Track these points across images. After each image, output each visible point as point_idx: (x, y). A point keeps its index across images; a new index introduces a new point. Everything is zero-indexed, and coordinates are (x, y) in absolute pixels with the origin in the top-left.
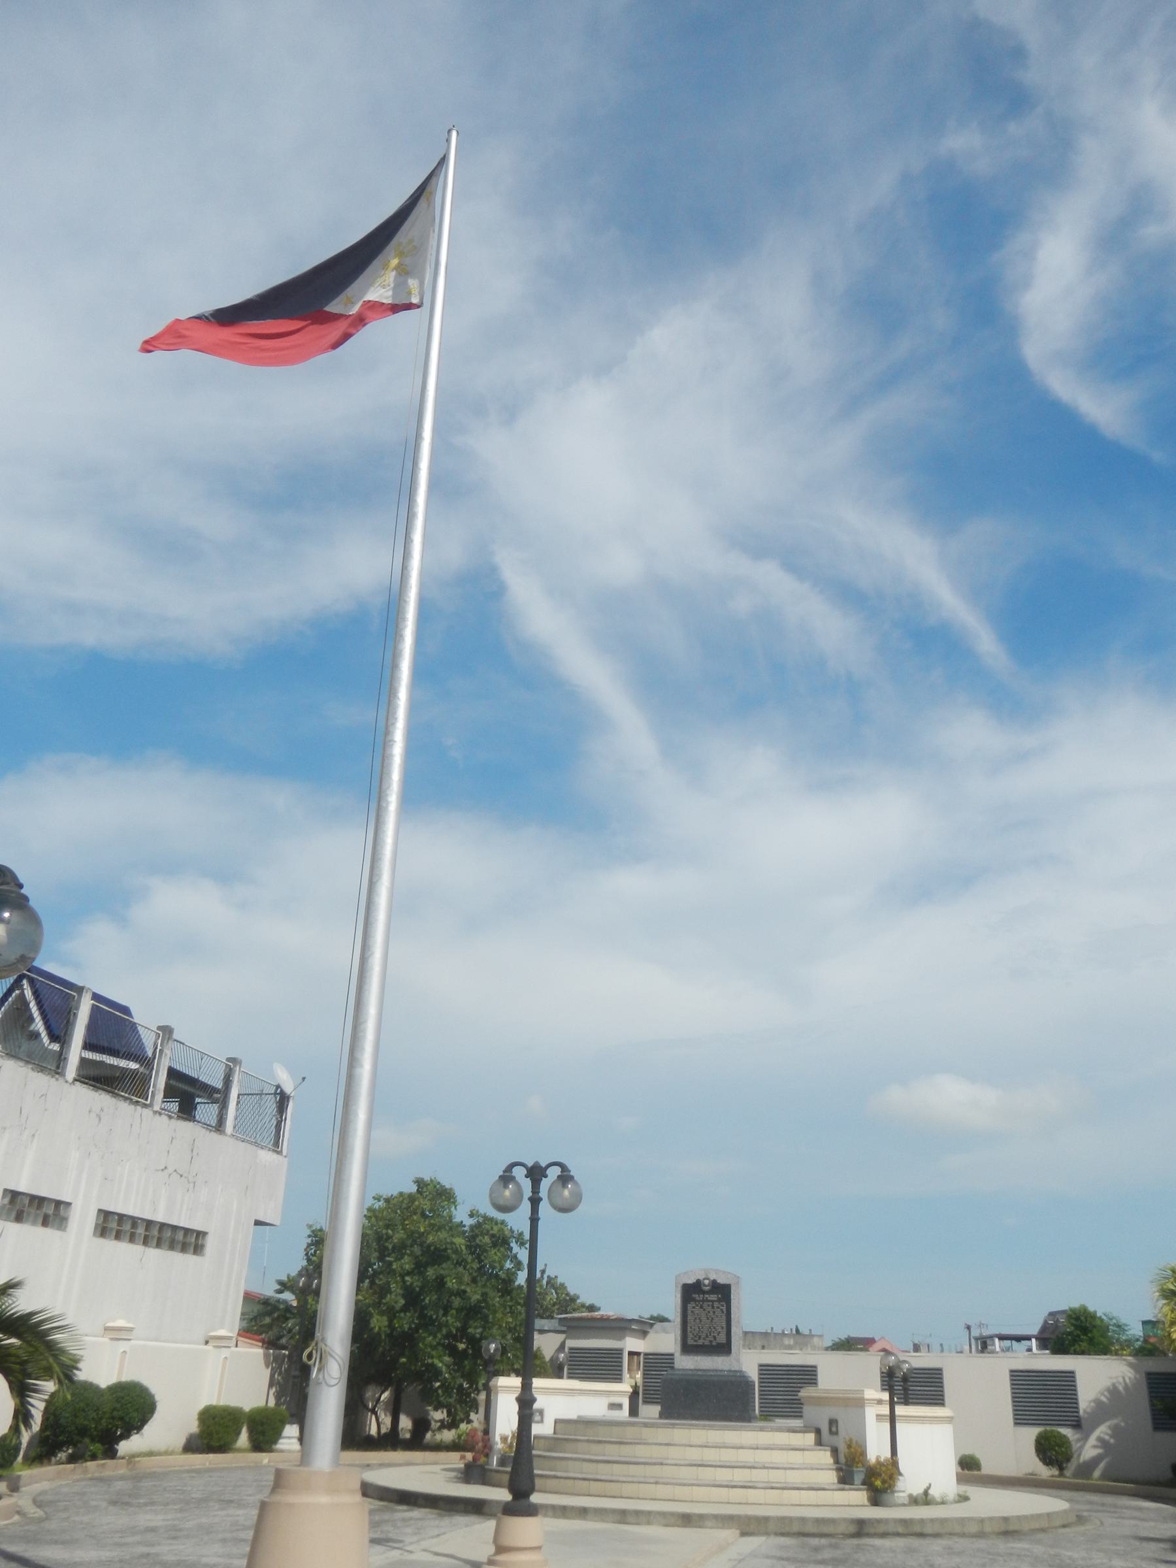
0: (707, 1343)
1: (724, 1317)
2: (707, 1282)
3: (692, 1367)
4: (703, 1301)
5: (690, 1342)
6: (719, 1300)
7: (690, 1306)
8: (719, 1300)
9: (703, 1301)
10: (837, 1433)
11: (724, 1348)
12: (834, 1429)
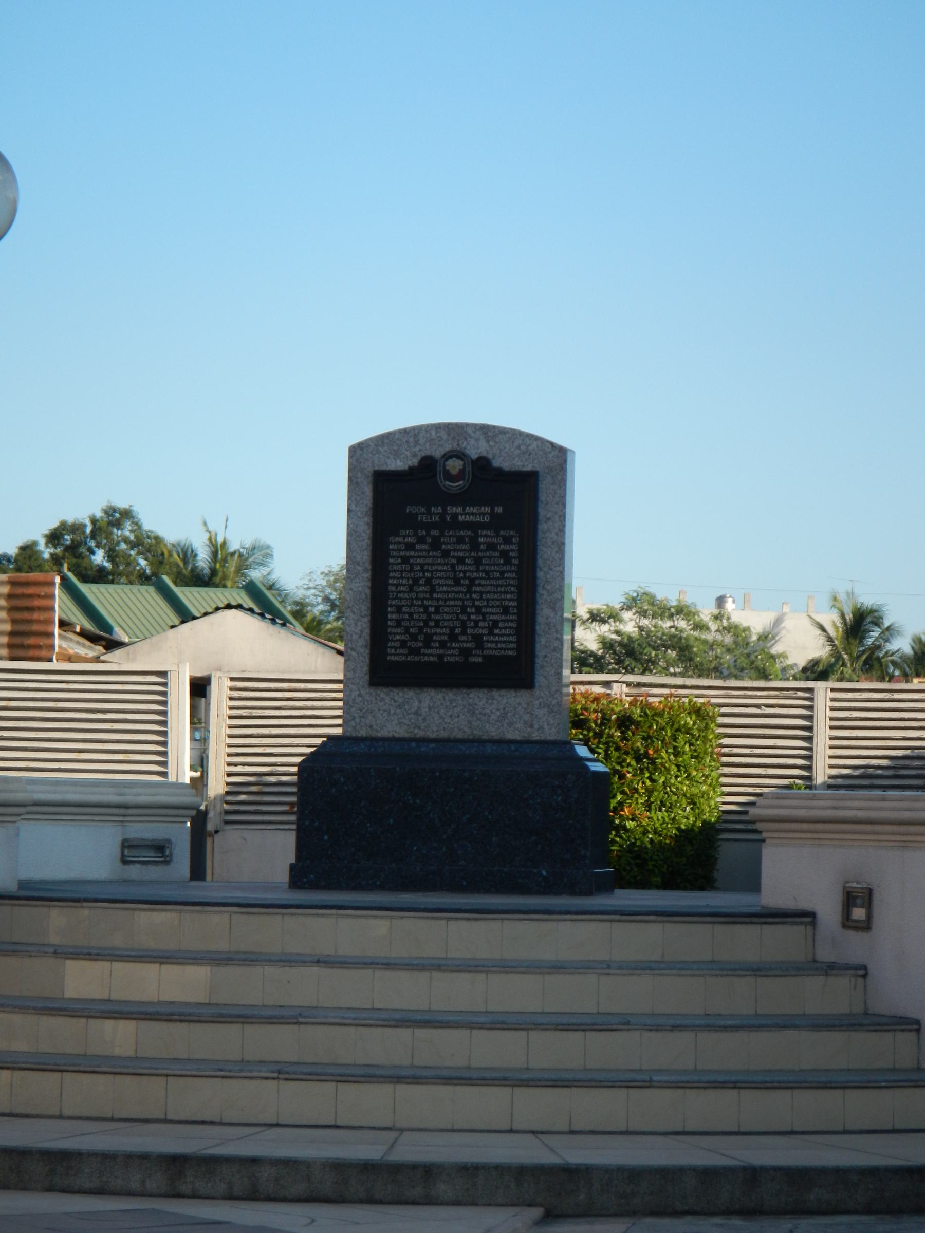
0: (452, 656)
2: (454, 466)
3: (401, 732)
4: (442, 525)
5: (396, 655)
6: (496, 523)
7: (395, 544)
8: (496, 523)
9: (442, 525)
10: (866, 926)
12: (858, 913)
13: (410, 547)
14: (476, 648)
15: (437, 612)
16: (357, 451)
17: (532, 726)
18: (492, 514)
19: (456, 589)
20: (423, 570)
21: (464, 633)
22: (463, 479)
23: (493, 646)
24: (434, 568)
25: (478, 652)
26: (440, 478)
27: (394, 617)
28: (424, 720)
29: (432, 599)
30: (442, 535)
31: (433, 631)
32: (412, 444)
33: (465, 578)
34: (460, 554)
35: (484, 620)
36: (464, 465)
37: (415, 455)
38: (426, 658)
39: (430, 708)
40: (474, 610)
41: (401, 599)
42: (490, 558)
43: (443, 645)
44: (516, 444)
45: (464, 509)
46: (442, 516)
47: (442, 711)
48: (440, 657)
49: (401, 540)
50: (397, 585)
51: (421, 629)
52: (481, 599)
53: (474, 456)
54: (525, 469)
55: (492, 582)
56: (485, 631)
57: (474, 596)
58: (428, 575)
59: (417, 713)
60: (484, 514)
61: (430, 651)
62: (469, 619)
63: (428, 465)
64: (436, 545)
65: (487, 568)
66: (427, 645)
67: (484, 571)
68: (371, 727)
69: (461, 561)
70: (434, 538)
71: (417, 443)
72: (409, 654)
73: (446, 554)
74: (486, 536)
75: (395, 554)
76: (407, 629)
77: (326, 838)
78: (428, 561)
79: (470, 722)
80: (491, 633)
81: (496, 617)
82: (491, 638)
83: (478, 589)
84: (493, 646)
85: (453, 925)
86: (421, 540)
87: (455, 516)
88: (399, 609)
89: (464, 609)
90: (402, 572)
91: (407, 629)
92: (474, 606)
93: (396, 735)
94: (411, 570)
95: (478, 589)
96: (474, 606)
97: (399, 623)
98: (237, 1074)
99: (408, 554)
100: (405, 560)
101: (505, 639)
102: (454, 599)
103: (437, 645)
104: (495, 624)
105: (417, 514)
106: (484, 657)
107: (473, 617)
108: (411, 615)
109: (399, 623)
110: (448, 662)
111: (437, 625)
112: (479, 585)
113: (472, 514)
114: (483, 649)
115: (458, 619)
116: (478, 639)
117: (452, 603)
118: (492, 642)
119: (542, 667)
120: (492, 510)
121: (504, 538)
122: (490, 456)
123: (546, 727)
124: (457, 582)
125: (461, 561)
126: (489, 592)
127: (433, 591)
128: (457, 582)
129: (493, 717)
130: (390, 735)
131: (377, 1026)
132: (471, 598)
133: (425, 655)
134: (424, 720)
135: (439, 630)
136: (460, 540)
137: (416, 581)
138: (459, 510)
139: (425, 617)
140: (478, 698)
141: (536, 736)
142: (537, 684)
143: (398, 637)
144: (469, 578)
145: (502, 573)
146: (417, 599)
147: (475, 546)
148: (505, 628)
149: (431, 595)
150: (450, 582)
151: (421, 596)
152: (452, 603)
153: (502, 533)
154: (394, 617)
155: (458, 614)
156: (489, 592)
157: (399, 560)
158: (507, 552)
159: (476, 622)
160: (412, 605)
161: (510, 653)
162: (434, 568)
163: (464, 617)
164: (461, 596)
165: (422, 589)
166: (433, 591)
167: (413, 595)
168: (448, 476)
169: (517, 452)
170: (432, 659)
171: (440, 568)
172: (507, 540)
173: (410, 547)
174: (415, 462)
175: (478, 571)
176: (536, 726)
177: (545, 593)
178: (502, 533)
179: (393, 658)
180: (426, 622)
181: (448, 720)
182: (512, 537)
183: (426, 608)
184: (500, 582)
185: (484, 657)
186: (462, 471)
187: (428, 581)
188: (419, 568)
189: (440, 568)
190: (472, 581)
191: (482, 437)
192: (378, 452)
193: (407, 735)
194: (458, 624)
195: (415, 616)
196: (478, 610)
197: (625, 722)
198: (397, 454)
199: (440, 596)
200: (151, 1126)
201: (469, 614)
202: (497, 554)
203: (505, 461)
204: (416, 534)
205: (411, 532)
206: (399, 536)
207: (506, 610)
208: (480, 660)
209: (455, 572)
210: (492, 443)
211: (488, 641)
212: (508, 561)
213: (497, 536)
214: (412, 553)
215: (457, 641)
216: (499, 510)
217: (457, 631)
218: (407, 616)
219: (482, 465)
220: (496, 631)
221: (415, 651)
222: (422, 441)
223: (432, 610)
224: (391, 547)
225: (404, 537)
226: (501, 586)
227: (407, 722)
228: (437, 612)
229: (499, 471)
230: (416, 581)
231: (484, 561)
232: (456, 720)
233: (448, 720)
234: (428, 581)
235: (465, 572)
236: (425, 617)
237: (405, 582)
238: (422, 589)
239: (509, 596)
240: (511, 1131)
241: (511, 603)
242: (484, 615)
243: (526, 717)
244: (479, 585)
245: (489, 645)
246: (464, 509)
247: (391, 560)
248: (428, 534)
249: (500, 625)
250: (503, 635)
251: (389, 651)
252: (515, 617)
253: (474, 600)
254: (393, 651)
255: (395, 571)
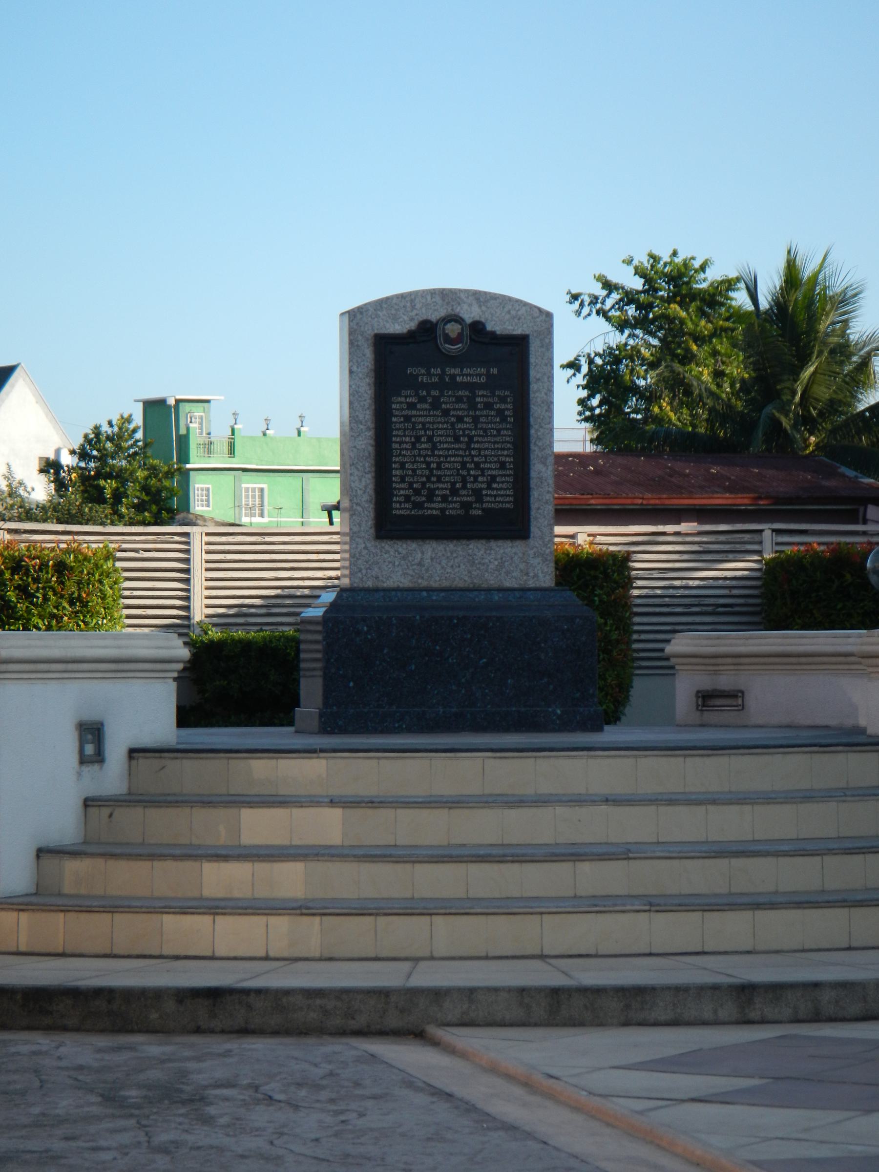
0: (453, 510)
1: (507, 435)
2: (453, 329)
3: (406, 582)
4: (442, 386)
5: (400, 509)
6: (492, 384)
7: (398, 404)
8: (492, 384)
9: (442, 386)
11: (513, 524)
13: (412, 406)
14: (476, 502)
15: (439, 468)
16: (355, 318)
17: (527, 574)
18: (488, 375)
19: (457, 446)
20: (425, 429)
21: (464, 487)
22: (461, 342)
23: (492, 499)
24: (435, 426)
25: (478, 505)
26: (440, 340)
27: (398, 473)
28: (427, 570)
29: (433, 455)
30: (442, 395)
31: (435, 486)
32: (409, 309)
33: (464, 435)
34: (460, 413)
35: (483, 475)
36: (462, 329)
37: (412, 319)
38: (429, 512)
39: (432, 559)
40: (473, 466)
41: (405, 456)
42: (487, 416)
43: (445, 499)
44: (506, 309)
45: (462, 370)
46: (441, 377)
47: (444, 562)
48: (443, 510)
49: (403, 399)
50: (400, 443)
51: (424, 484)
52: (480, 455)
53: (469, 321)
54: (515, 333)
55: (489, 439)
56: (484, 486)
57: (473, 452)
58: (429, 433)
59: (420, 564)
60: (480, 375)
61: (433, 505)
62: (469, 474)
63: (427, 331)
64: (436, 404)
65: (484, 426)
66: (430, 497)
67: (481, 429)
68: (377, 578)
69: (460, 419)
70: (434, 397)
71: (413, 307)
72: (414, 508)
73: (446, 413)
74: (483, 396)
75: (397, 413)
76: (411, 484)
77: (351, 684)
78: (428, 419)
79: (470, 572)
80: (489, 487)
81: (493, 473)
82: (490, 492)
83: (476, 446)
84: (492, 499)
85: (689, 760)
86: (422, 400)
87: (453, 377)
88: (402, 466)
89: (464, 464)
90: (405, 430)
91: (411, 484)
92: (473, 462)
93: (401, 585)
94: (414, 428)
95: (476, 446)
96: (473, 462)
97: (403, 480)
98: (611, 909)
99: (410, 413)
100: (407, 419)
101: (502, 492)
102: (455, 456)
103: (439, 499)
104: (493, 478)
105: (418, 375)
106: (483, 510)
107: (472, 472)
108: (414, 470)
109: (403, 480)
110: (451, 516)
111: (439, 480)
112: (478, 442)
113: (470, 375)
114: (482, 502)
115: (458, 475)
116: (477, 493)
117: (452, 459)
118: (491, 496)
119: (536, 518)
120: (488, 371)
121: (499, 396)
122: (483, 320)
123: (540, 575)
124: (457, 439)
125: (460, 419)
126: (487, 449)
127: (434, 447)
128: (457, 439)
129: (491, 566)
130: (395, 585)
131: (698, 858)
132: (470, 455)
133: (428, 508)
134: (427, 570)
135: (441, 486)
136: (459, 400)
137: (418, 439)
138: (457, 371)
139: (427, 472)
140: (477, 549)
141: (531, 584)
142: (532, 535)
143: (402, 492)
144: (468, 436)
145: (499, 431)
146: (419, 455)
147: (473, 406)
148: (503, 482)
149: (433, 451)
150: (450, 439)
151: (423, 453)
152: (452, 459)
153: (497, 393)
154: (398, 473)
155: (458, 470)
156: (487, 449)
157: (402, 419)
158: (504, 410)
159: (476, 477)
160: (415, 462)
161: (508, 506)
162: (435, 426)
163: (464, 473)
164: (461, 453)
165: (424, 446)
166: (434, 447)
167: (416, 452)
168: (448, 340)
169: (508, 317)
170: (434, 512)
171: (440, 426)
172: (503, 400)
173: (412, 406)
174: (413, 325)
175: (476, 429)
176: (532, 574)
177: (536, 449)
178: (497, 393)
179: (398, 512)
180: (428, 478)
181: (449, 570)
182: (507, 396)
183: (428, 464)
184: (497, 439)
185: (483, 510)
186: (460, 335)
187: (430, 439)
188: (420, 426)
189: (440, 426)
190: (471, 438)
191: (474, 302)
192: (377, 316)
193: (411, 585)
194: (459, 479)
195: (418, 472)
196: (477, 465)
197: (61, 567)
198: (395, 318)
199: (441, 453)
200: (300, 965)
201: (469, 470)
202: (493, 413)
203: (498, 324)
204: (417, 394)
205: (412, 392)
206: (401, 396)
207: (503, 466)
208: (480, 512)
209: (454, 429)
210: (484, 308)
211: (487, 495)
212: (504, 419)
213: (493, 395)
214: (414, 412)
215: (458, 495)
216: (494, 371)
217: (458, 486)
218: (410, 472)
219: (477, 327)
220: (495, 486)
221: (418, 505)
222: (418, 306)
223: (433, 466)
224: (393, 406)
225: (406, 397)
226: (498, 443)
227: (411, 572)
228: (439, 468)
229: (493, 333)
230: (418, 439)
231: (481, 420)
232: (457, 570)
233: (449, 570)
234: (430, 439)
235: (464, 430)
236: (427, 472)
237: (408, 439)
238: (424, 446)
239: (505, 453)
240: (849, 949)
241: (508, 459)
242: (483, 470)
243: (522, 566)
244: (478, 442)
245: (488, 499)
246: (462, 370)
247: (394, 419)
248: (428, 394)
249: (498, 479)
250: (501, 489)
251: (394, 505)
252: (511, 472)
253: (473, 456)
254: (398, 506)
255: (398, 429)
